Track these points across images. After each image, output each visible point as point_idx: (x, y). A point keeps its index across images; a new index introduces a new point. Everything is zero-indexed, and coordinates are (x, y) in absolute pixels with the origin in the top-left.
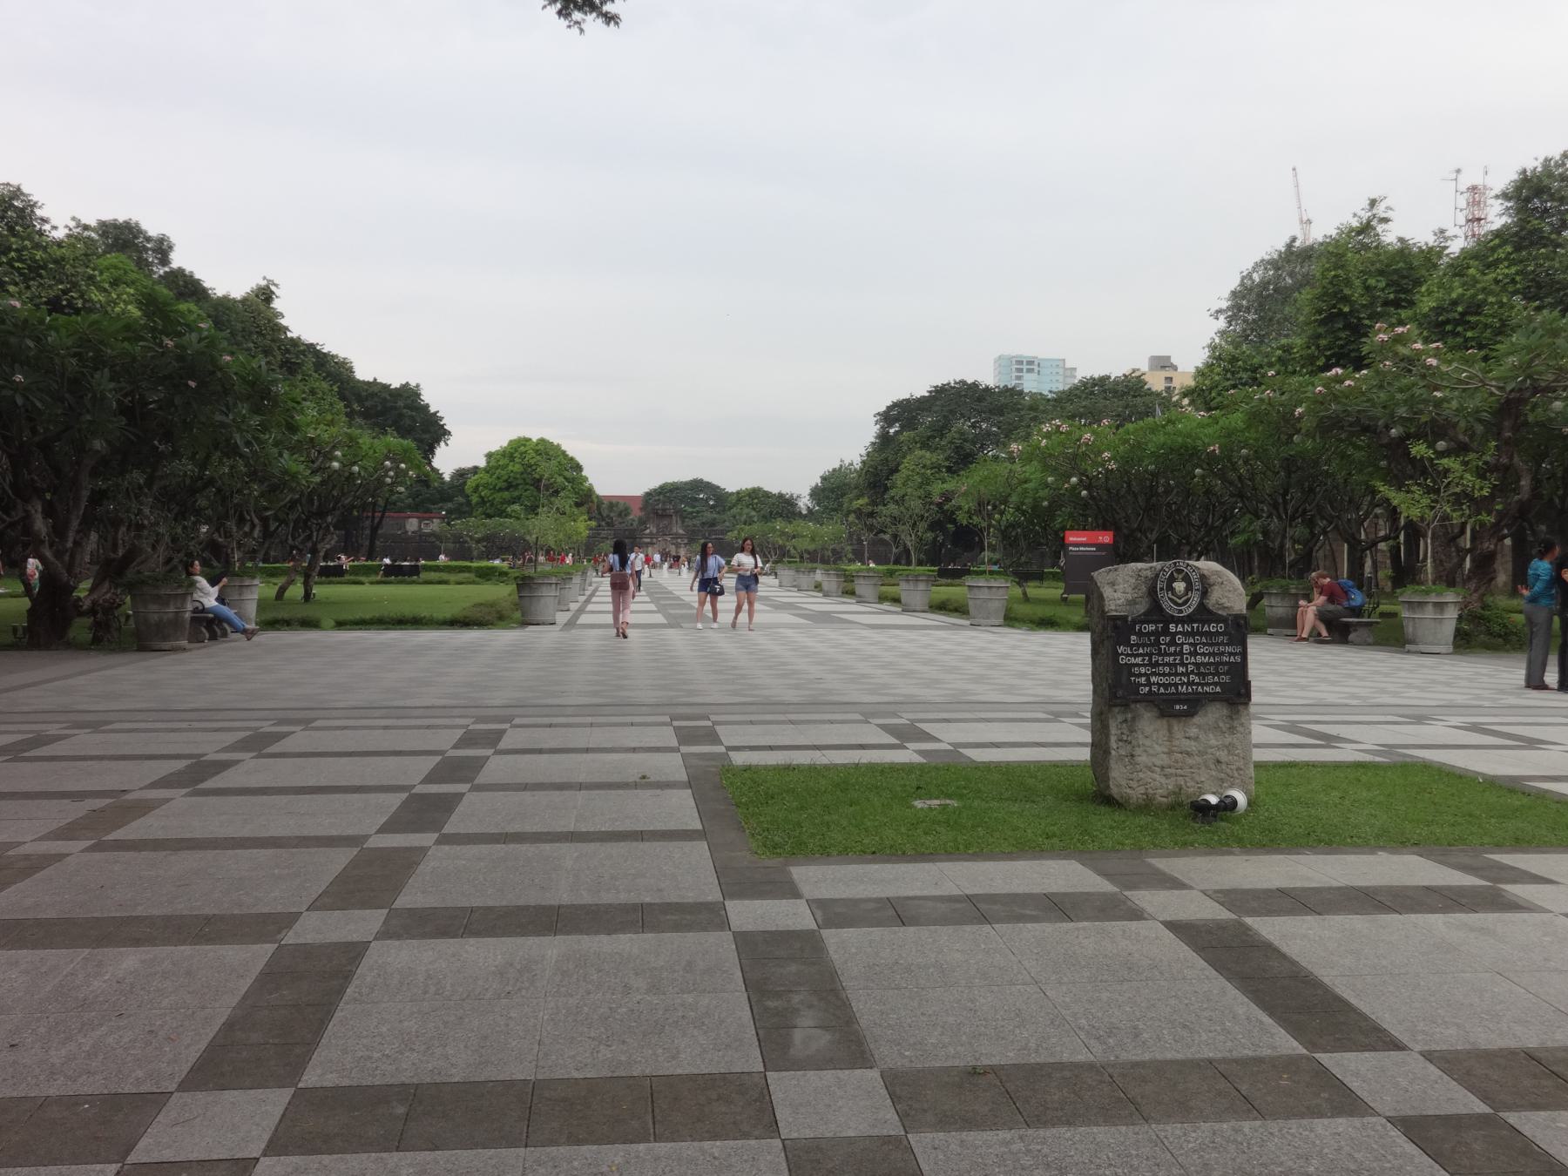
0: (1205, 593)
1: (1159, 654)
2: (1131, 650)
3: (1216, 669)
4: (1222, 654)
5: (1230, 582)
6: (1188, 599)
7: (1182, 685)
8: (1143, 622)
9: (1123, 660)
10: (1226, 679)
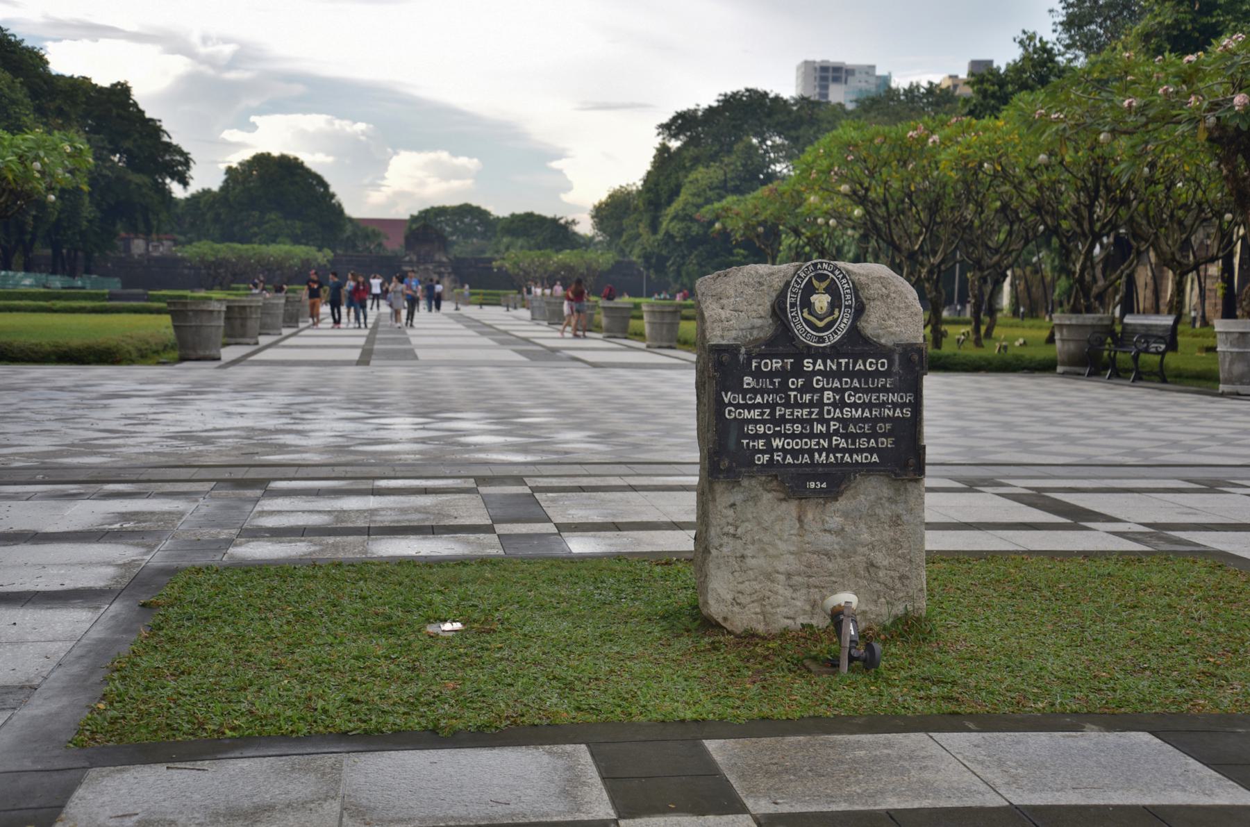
0: (860, 310)
1: (787, 405)
2: (744, 399)
3: (873, 428)
4: (883, 405)
5: (900, 293)
6: (835, 321)
7: (820, 452)
8: (762, 356)
9: (730, 414)
10: (886, 443)
